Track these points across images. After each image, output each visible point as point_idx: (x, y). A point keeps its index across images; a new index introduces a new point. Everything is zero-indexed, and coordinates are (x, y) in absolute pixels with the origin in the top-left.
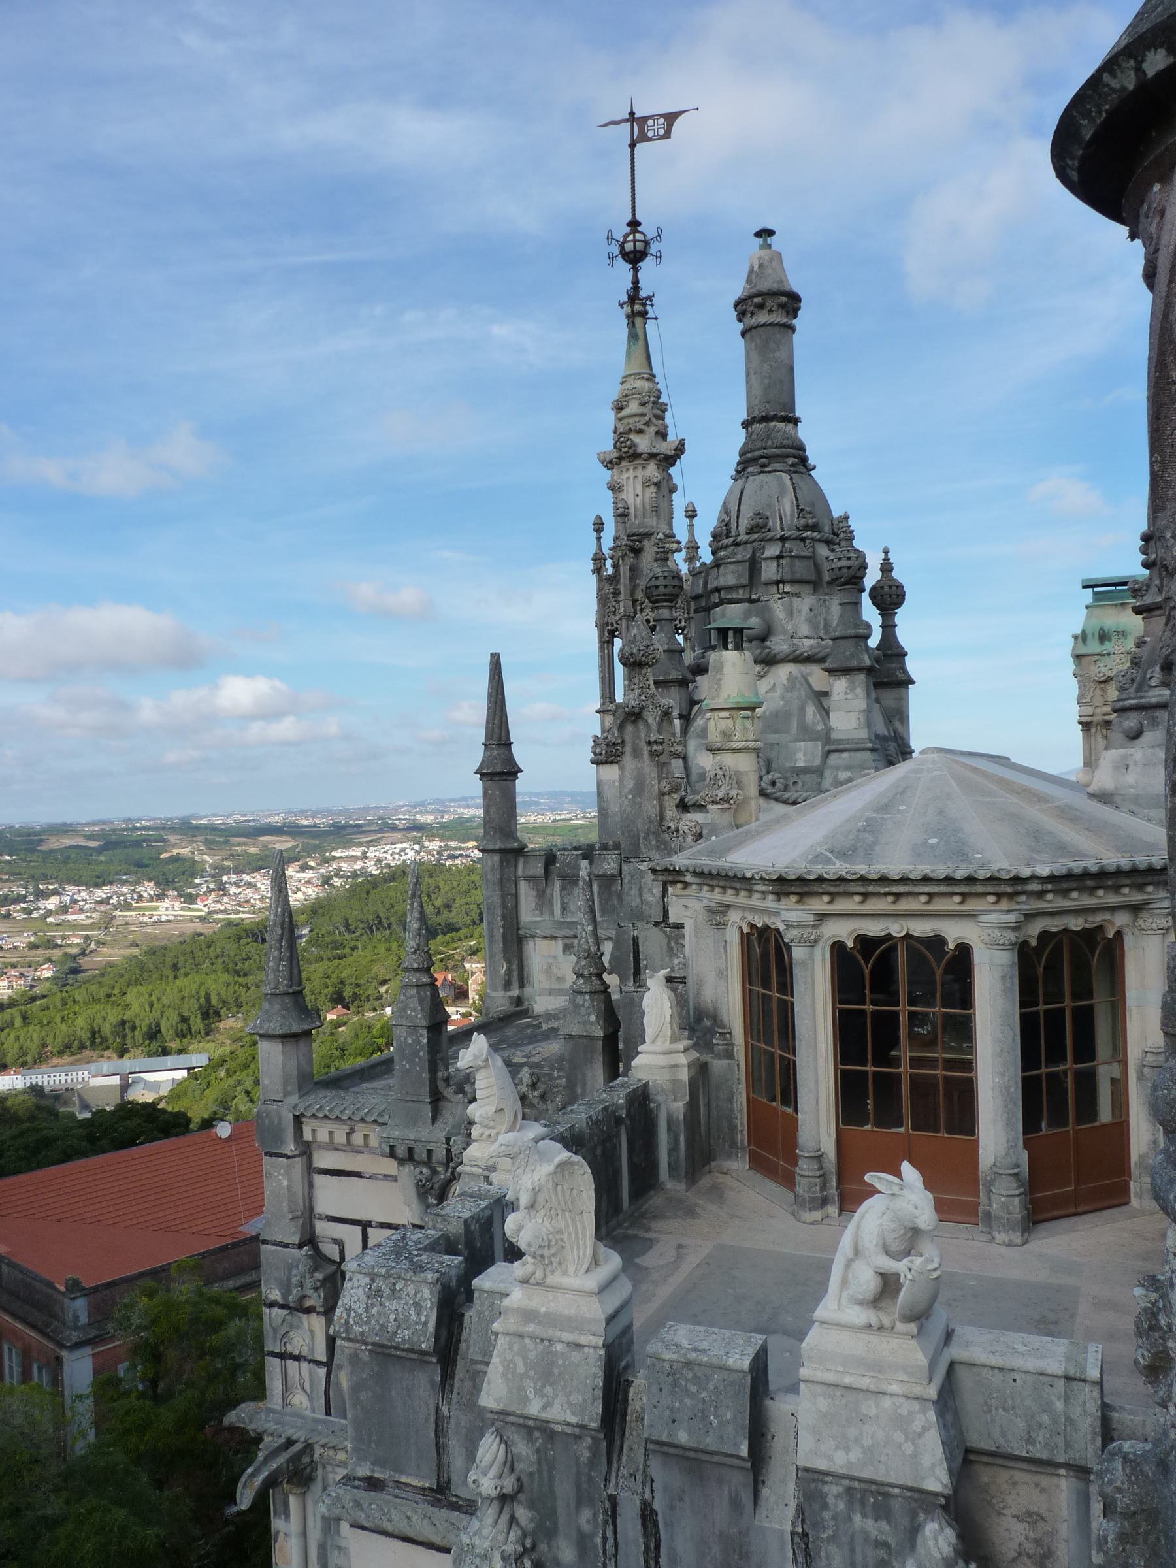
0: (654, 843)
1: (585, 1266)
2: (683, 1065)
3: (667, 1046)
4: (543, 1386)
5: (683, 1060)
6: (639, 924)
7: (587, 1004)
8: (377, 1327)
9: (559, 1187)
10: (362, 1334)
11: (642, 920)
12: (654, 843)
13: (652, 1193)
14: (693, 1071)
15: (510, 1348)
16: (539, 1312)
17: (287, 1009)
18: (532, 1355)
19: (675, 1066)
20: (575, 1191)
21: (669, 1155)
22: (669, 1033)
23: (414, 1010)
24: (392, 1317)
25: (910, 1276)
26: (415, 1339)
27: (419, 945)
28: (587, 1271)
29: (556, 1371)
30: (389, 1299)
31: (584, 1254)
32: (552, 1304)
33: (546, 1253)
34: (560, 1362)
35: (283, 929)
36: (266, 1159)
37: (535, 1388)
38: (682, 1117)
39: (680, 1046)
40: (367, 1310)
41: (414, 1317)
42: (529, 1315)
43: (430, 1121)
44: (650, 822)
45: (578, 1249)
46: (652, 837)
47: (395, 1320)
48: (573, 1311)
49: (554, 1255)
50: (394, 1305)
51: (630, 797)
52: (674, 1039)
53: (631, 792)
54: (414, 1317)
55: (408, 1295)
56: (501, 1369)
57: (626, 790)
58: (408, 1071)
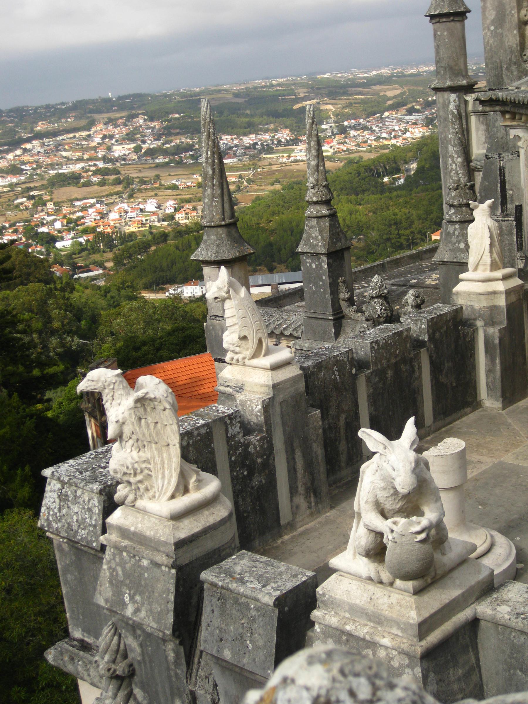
0: (515, 73)
1: (169, 493)
2: (501, 292)
3: (484, 272)
4: (135, 594)
5: (500, 286)
6: (504, 155)
7: (457, 233)
8: (66, 525)
9: (143, 421)
10: (57, 529)
11: (507, 150)
12: (515, 73)
13: (468, 410)
14: (513, 298)
15: (114, 559)
16: (129, 530)
17: (221, 239)
18: (128, 566)
19: (494, 293)
20: (159, 425)
21: (487, 376)
22: (489, 262)
23: (316, 238)
24: (75, 518)
25: (390, 537)
26: (89, 538)
27: (317, 180)
28: (173, 497)
29: (143, 583)
30: (73, 503)
31: (169, 483)
32: (140, 525)
33: (132, 480)
34: (146, 575)
35: (213, 170)
36: (216, 363)
37: (129, 594)
38: (497, 341)
39: (499, 274)
40: (60, 509)
41: (88, 520)
42: (124, 532)
43: (333, 335)
44: (512, 52)
45: (163, 477)
46: (514, 68)
47: (77, 521)
48: (152, 533)
49: (140, 482)
50: (75, 508)
51: (492, 28)
52: (494, 266)
53: (493, 22)
54: (88, 520)
55: (84, 501)
56: (108, 574)
57: (488, 22)
58: (314, 292)
